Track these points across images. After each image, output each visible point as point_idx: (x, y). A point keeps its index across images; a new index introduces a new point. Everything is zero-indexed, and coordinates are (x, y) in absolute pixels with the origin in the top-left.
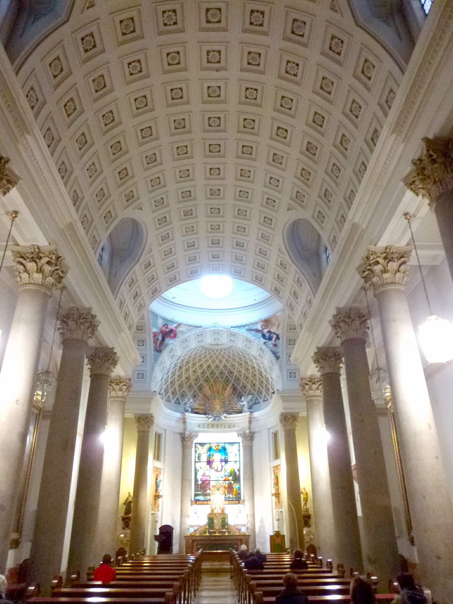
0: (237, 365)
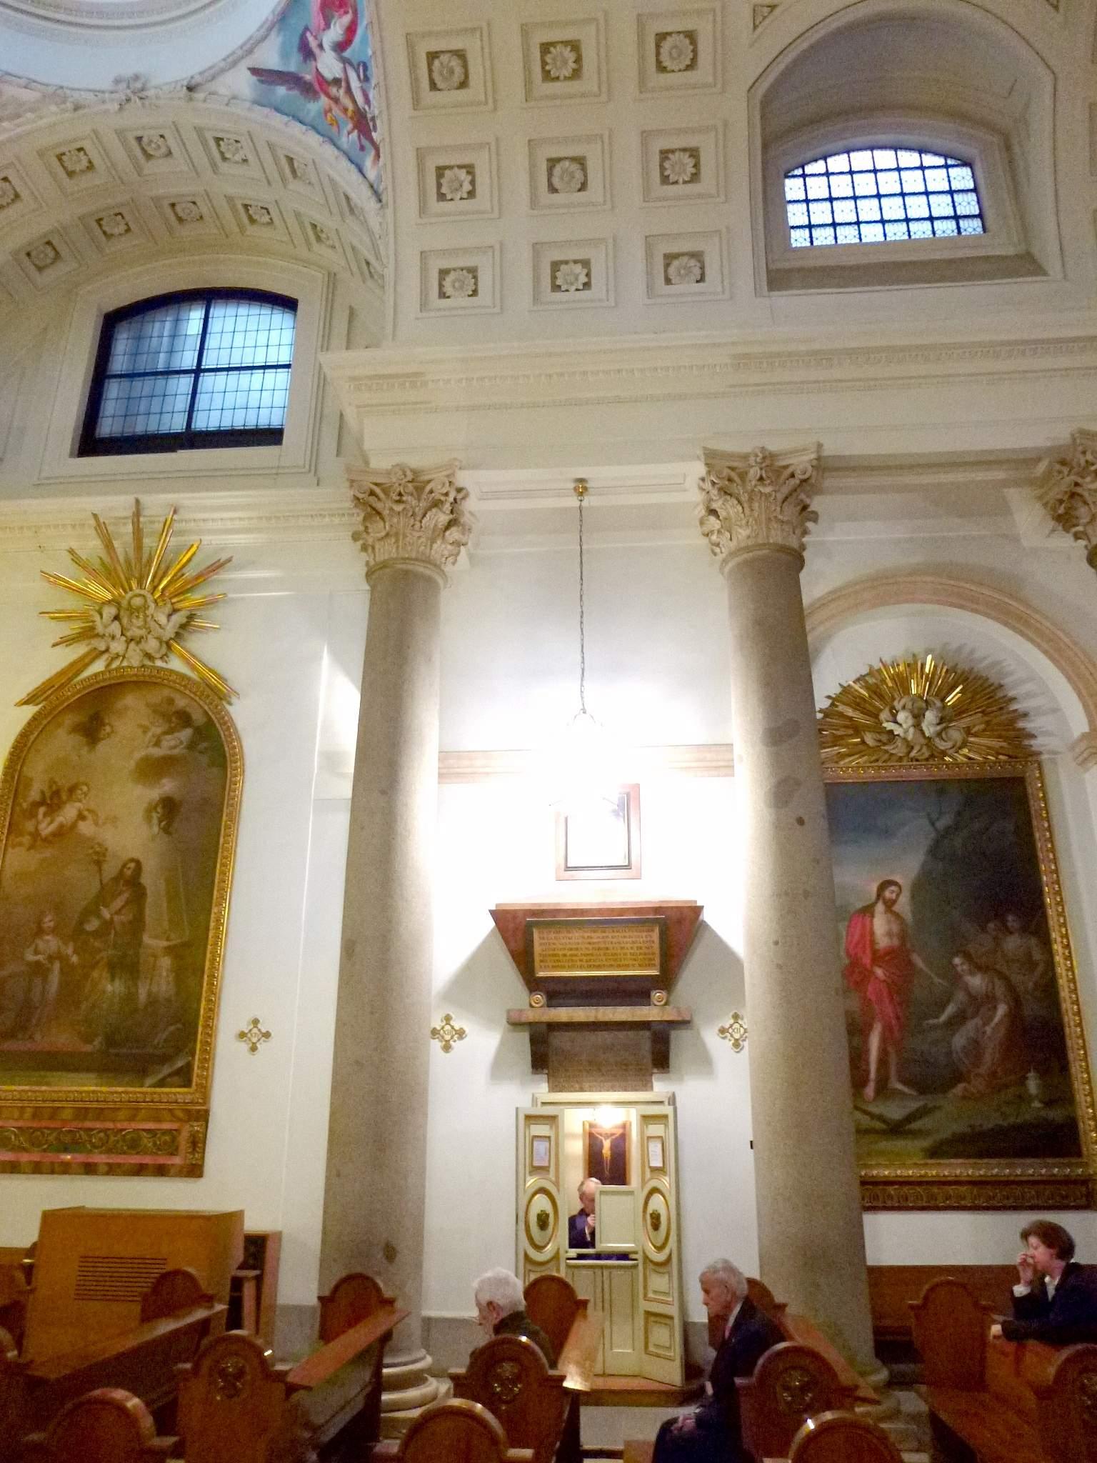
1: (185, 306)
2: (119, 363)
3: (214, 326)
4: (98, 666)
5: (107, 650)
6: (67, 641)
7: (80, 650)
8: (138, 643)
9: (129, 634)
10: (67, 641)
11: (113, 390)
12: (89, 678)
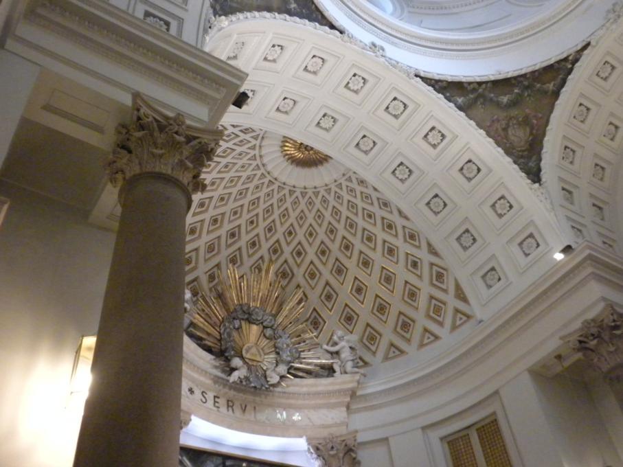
0: (311, 254)
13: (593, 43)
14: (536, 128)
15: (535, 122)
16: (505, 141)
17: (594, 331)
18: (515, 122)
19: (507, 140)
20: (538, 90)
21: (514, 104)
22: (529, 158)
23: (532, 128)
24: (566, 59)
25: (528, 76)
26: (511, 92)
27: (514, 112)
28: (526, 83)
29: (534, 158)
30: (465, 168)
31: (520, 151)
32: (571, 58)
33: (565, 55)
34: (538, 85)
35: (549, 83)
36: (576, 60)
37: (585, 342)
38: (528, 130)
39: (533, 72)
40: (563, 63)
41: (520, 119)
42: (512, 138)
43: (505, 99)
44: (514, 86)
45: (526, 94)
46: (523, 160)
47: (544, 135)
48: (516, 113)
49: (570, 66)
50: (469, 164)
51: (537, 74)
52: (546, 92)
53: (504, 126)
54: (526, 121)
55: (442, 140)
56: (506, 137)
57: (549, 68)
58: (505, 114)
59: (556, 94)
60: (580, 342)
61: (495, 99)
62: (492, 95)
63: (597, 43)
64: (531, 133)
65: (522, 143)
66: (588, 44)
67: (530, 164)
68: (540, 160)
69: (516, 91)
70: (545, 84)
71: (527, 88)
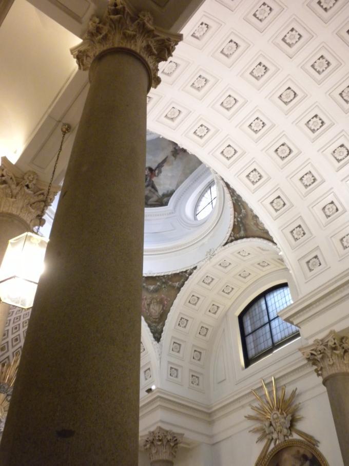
1: (259, 302)
2: (249, 329)
3: (269, 304)
4: (272, 446)
5: (272, 439)
6: (260, 439)
7: (265, 441)
8: (281, 432)
9: (277, 430)
10: (260, 439)
11: (250, 339)
12: (272, 450)
13: (198, 268)
14: (166, 306)
15: (166, 303)
16: (147, 311)
17: (320, 348)
18: (155, 301)
19: (149, 311)
20: (170, 285)
21: (156, 291)
22: (159, 323)
23: (164, 306)
24: (186, 272)
25: (166, 277)
26: (156, 284)
27: (156, 295)
28: (164, 280)
29: (161, 324)
30: (275, 202)
31: (154, 319)
32: (188, 271)
33: (184, 270)
34: (170, 283)
35: (176, 282)
36: (190, 274)
37: (315, 355)
38: (161, 307)
39: (168, 275)
40: (184, 273)
41: (158, 300)
42: (152, 310)
43: (152, 288)
44: (158, 281)
45: (163, 286)
46: (154, 324)
47: (169, 311)
48: (157, 296)
49: (187, 276)
50: (278, 200)
51: (170, 276)
52: (174, 287)
53: (148, 303)
54: (161, 302)
55: (259, 180)
56: (149, 310)
57: (176, 275)
58: (150, 296)
59: (179, 289)
60: (312, 354)
61: (146, 287)
62: (145, 284)
63: (200, 268)
64: (163, 308)
65: (157, 314)
66: (195, 268)
67: (158, 327)
68: (164, 325)
69: (158, 284)
70: (173, 282)
71: (164, 283)
